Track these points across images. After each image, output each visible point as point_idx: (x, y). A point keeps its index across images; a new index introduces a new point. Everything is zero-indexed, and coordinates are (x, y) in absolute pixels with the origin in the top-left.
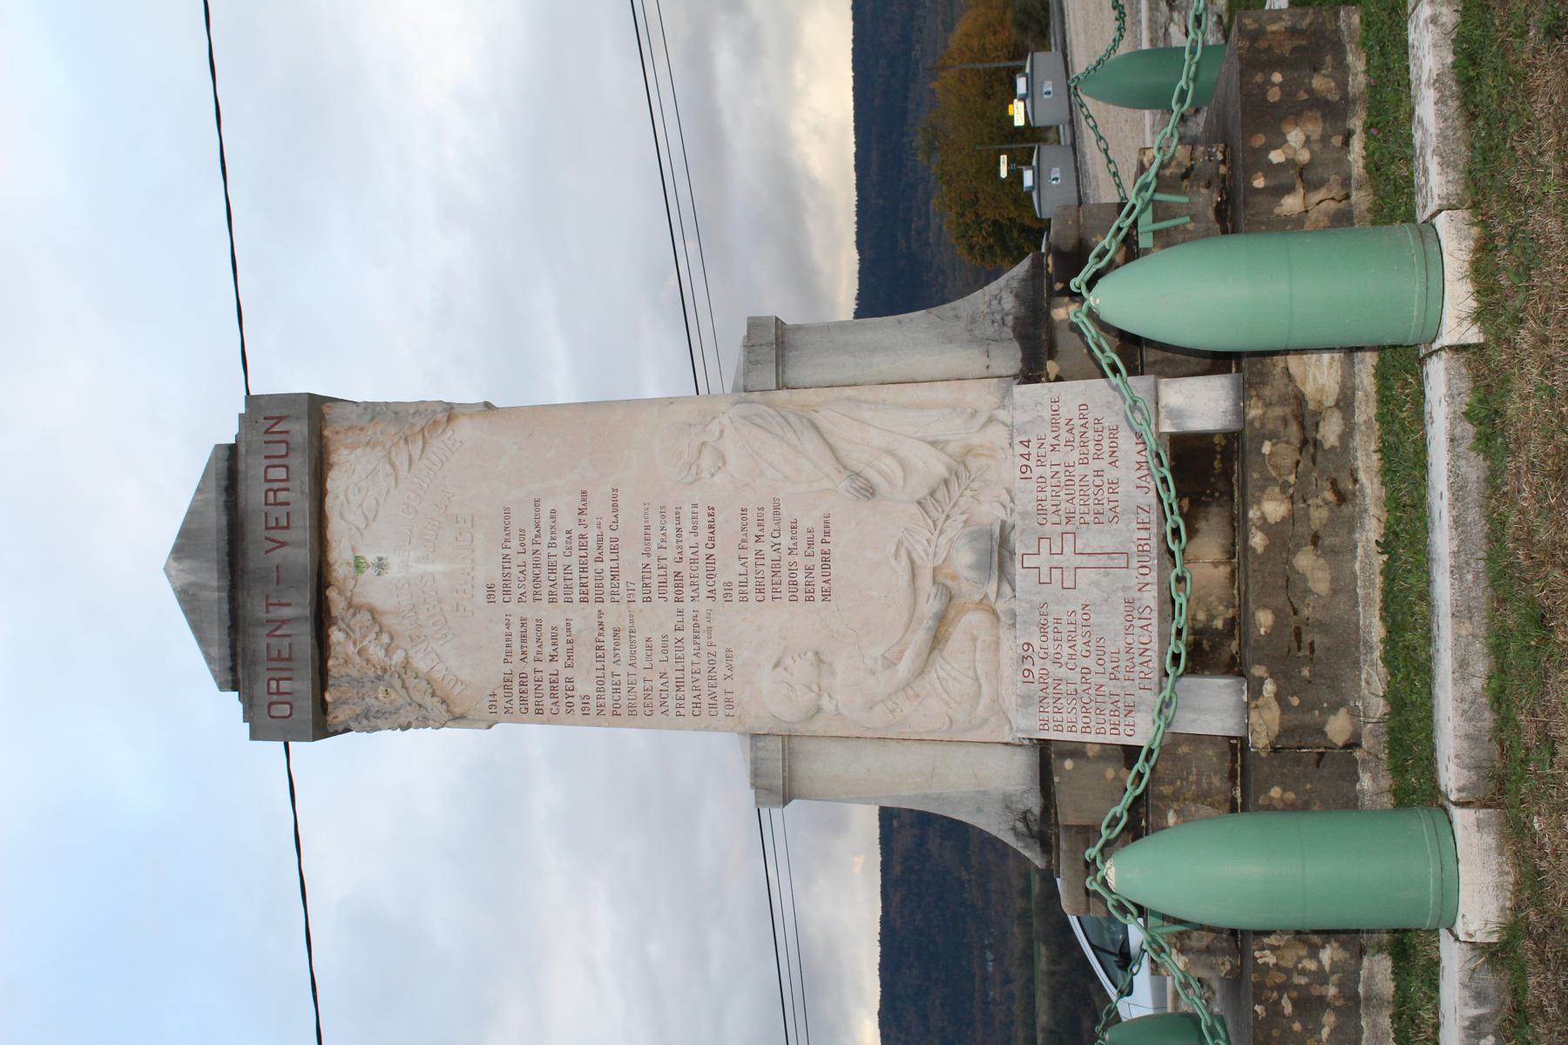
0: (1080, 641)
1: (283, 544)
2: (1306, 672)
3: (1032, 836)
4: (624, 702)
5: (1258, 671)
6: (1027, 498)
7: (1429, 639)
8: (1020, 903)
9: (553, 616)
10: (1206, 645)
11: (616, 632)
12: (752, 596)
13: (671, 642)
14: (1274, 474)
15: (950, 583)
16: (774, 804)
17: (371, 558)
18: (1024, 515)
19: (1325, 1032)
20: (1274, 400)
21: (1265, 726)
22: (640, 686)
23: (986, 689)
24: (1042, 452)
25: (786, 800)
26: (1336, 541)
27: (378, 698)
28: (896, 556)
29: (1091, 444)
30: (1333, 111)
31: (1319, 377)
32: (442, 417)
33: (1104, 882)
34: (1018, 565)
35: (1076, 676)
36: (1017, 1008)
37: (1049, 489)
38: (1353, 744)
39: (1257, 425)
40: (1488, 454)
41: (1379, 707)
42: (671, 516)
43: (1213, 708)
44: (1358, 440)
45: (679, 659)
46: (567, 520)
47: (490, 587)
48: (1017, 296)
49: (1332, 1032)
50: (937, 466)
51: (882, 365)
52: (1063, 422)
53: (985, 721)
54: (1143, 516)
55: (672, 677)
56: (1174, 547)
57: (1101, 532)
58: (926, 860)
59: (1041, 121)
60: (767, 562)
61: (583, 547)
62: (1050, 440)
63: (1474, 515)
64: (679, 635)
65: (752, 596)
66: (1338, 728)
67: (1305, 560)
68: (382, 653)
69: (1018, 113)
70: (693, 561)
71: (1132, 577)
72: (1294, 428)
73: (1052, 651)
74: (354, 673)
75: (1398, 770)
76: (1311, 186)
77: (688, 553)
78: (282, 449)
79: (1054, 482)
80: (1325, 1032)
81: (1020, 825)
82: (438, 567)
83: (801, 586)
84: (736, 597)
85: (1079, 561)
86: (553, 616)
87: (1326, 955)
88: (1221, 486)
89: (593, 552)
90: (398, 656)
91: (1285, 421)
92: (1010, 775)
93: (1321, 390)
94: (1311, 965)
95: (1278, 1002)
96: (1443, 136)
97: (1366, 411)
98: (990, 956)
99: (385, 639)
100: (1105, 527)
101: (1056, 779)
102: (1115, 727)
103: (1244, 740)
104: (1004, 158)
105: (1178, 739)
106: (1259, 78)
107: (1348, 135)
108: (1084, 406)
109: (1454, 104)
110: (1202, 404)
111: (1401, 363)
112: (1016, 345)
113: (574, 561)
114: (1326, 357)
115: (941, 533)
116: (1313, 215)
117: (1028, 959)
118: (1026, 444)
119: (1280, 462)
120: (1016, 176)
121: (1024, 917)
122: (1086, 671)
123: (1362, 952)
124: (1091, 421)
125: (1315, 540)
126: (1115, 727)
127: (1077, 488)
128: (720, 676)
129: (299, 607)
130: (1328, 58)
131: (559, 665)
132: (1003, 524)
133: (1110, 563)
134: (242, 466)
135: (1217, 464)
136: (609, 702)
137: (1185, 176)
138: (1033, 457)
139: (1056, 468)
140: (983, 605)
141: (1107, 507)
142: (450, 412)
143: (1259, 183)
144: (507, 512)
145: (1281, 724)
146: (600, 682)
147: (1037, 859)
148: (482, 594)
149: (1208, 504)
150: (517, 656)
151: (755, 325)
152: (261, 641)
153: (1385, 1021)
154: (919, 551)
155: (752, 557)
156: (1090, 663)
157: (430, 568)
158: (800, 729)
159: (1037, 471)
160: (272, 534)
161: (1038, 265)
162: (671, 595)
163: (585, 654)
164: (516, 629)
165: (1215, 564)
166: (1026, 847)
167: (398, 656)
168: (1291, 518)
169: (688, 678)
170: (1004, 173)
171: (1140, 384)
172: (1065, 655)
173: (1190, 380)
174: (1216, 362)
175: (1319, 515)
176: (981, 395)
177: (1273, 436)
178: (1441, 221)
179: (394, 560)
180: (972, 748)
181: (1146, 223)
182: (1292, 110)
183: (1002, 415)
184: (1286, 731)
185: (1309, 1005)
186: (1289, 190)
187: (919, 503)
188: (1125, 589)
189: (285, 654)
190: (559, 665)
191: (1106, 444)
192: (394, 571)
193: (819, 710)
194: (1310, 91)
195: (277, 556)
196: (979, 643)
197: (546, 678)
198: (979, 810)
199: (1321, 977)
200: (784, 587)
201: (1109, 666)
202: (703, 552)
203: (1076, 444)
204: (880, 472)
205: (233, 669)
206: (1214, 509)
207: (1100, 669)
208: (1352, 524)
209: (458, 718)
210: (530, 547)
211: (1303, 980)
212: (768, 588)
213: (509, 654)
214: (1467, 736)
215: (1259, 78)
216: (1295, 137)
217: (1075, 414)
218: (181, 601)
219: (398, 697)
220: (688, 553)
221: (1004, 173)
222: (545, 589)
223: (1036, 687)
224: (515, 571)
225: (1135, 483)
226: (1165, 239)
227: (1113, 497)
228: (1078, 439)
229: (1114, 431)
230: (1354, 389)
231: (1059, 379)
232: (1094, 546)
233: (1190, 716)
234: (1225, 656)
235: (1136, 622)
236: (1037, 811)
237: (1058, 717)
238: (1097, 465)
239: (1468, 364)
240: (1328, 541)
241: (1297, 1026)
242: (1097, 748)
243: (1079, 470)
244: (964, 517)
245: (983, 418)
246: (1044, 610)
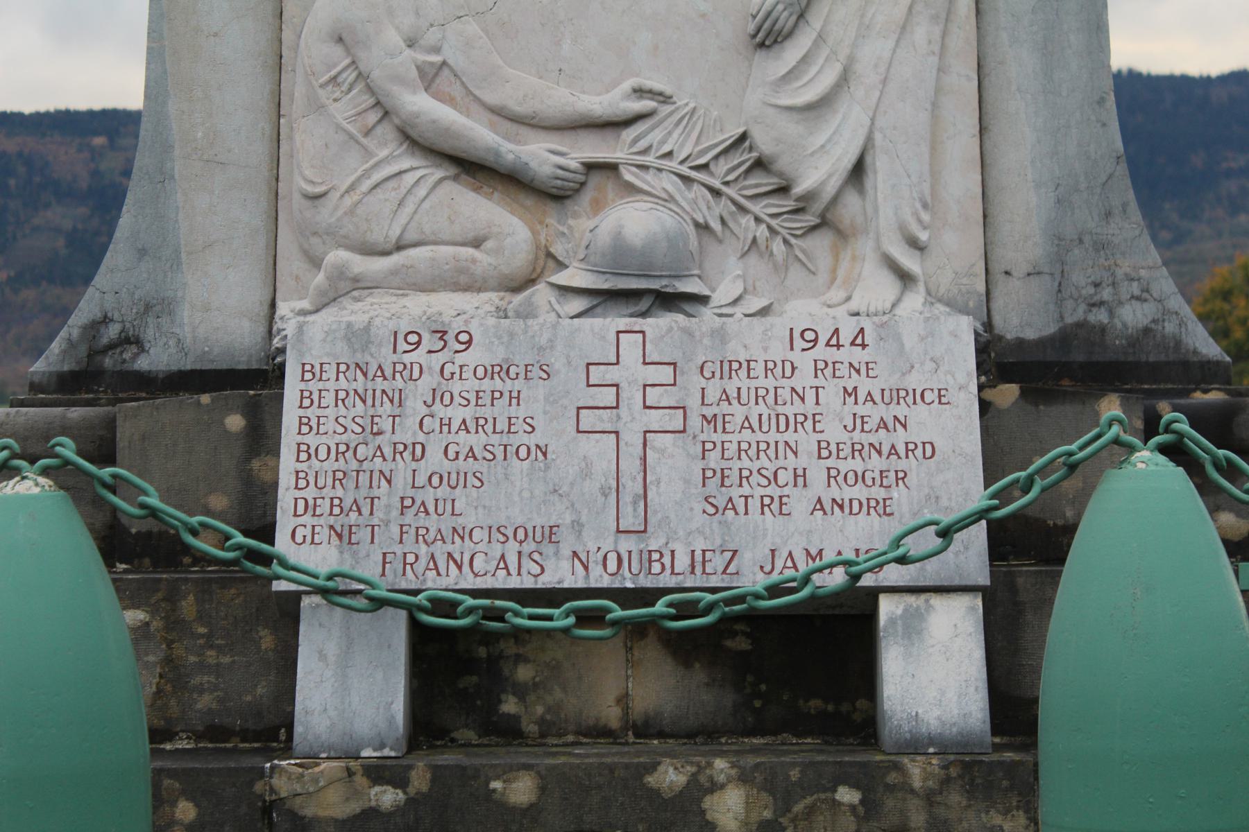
0: (477, 440)
3: (95, 353)
6: (753, 341)
14: (798, 808)
15: (587, 197)
18: (720, 336)
20: (941, 812)
24: (843, 370)
28: (639, 92)
29: (857, 464)
34: (623, 323)
35: (408, 433)
37: (770, 383)
39: (893, 777)
43: (349, 691)
48: (1147, 331)
50: (819, 171)
52: (901, 411)
54: (718, 562)
56: (660, 607)
57: (687, 482)
62: (865, 385)
71: (599, 539)
73: (456, 386)
79: (785, 394)
81: (113, 331)
85: (632, 438)
92: (211, 314)
100: (697, 490)
101: (205, 399)
102: (311, 508)
103: (287, 750)
105: (287, 613)
108: (930, 451)
110: (932, 673)
112: (1051, 329)
115: (686, 179)
118: (859, 341)
122: (418, 452)
124: (902, 464)
126: (311, 508)
127: (772, 437)
132: (702, 300)
133: (627, 498)
135: (815, 704)
138: (832, 354)
139: (810, 396)
141: (735, 492)
145: (316, 820)
147: (51, 360)
154: (653, 135)
159: (805, 362)
161: (1207, 373)
166: (71, 344)
171: (971, 555)
172: (450, 412)
173: (979, 654)
176: (956, 253)
187: (743, 137)
188: (577, 526)
191: (859, 492)
196: (470, 251)
198: (142, 252)
201: (429, 496)
203: (857, 436)
204: (805, 60)
206: (729, 699)
207: (421, 480)
223: (386, 357)
225: (778, 545)
227: (754, 504)
228: (866, 439)
229: (883, 509)
231: (985, 406)
232: (659, 468)
233: (332, 649)
235: (513, 547)
237: (329, 399)
238: (817, 475)
242: (267, 477)
243: (806, 441)
244: (716, 225)
245: (909, 261)
246: (536, 372)
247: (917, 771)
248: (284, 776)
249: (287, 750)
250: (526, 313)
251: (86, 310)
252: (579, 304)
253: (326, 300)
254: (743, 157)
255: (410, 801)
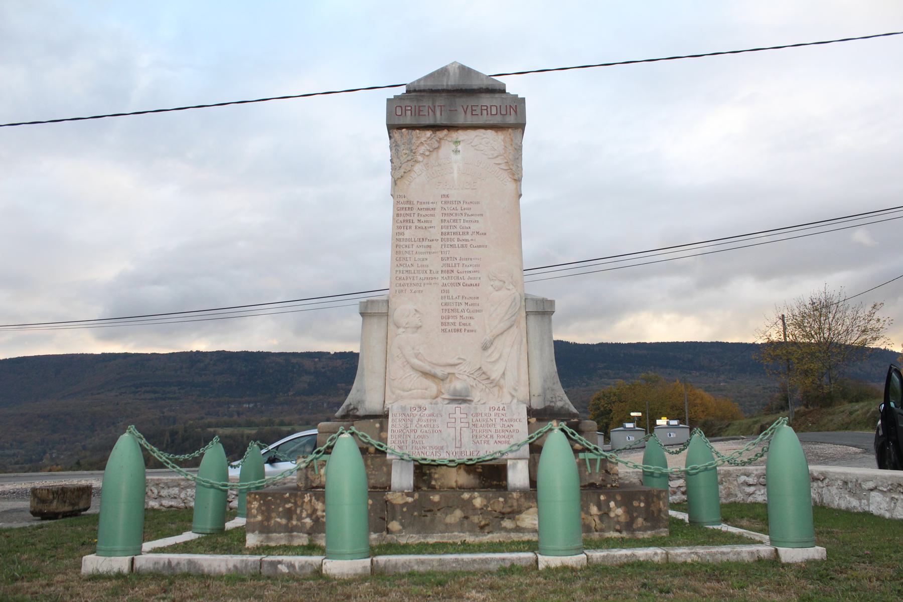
1: (465, 112)
2: (416, 513)
4: (401, 249)
5: (416, 495)
6: (481, 409)
7: (431, 553)
8: (277, 421)
9: (436, 221)
10: (425, 478)
11: (430, 247)
12: (444, 301)
13: (425, 269)
16: (360, 309)
17: (460, 147)
18: (476, 408)
19: (278, 520)
21: (395, 498)
22: (408, 256)
23: (406, 393)
25: (363, 314)
26: (466, 525)
27: (403, 150)
28: (459, 359)
30: (629, 526)
31: (529, 520)
32: (516, 177)
33: (342, 433)
35: (413, 427)
36: (225, 418)
38: (388, 531)
40: (499, 571)
41: (403, 541)
42: (477, 269)
44: (504, 534)
45: (419, 272)
46: (474, 227)
47: (447, 196)
49: (279, 523)
50: (495, 375)
51: (535, 353)
53: (393, 393)
54: (475, 453)
55: (412, 269)
58: (344, 368)
59: (657, 432)
60: (457, 307)
61: (464, 233)
63: (476, 566)
64: (428, 272)
65: (444, 301)
66: (395, 525)
67: (458, 513)
68: (421, 152)
69: (662, 422)
70: (458, 278)
71: (452, 449)
72: (508, 510)
74: (413, 141)
75: (380, 547)
76: (601, 517)
77: (461, 275)
78: (504, 112)
80: (278, 520)
81: (352, 407)
82: (456, 175)
83: (447, 321)
84: (443, 295)
86: (436, 221)
87: (308, 521)
88: (487, 484)
89: (461, 237)
90: (420, 158)
91: (512, 506)
93: (523, 520)
94: (304, 515)
95: (290, 502)
96: (614, 557)
97: (515, 537)
98: (251, 405)
99: (427, 153)
104: (640, 414)
106: (642, 498)
107: (620, 531)
108: (518, 431)
109: (625, 560)
110: (518, 476)
111: (533, 546)
112: (542, 407)
113: (458, 230)
114: (536, 522)
116: (590, 518)
117: (249, 425)
118: (504, 409)
119: (496, 504)
120: (631, 420)
121: (271, 423)
122: (416, 431)
123: (309, 534)
125: (466, 518)
128: (412, 288)
129: (440, 119)
130: (649, 524)
131: (416, 224)
134: (497, 95)
136: (402, 243)
137: (607, 471)
140: (440, 393)
142: (518, 181)
143: (602, 498)
144: (478, 203)
146: (410, 240)
147: (340, 412)
148: (444, 192)
149: (479, 479)
150: (420, 206)
151: (552, 303)
152: (426, 103)
153: (283, 542)
154: (462, 367)
155: (459, 301)
156: (419, 433)
157: (455, 171)
158: (390, 320)
160: (470, 108)
161: (574, 416)
162: (444, 269)
163: (420, 234)
164: (431, 206)
165: (456, 482)
167: (420, 158)
168: (474, 508)
169: (411, 275)
170: (633, 414)
174: (533, 483)
175: (475, 519)
176: (523, 392)
177: (506, 502)
178: (584, 556)
179: (459, 157)
180: (382, 388)
181: (588, 456)
182: (630, 511)
183: (515, 401)
184: (393, 506)
185: (289, 514)
186: (599, 509)
188: (447, 447)
189: (421, 113)
190: (416, 224)
191: (503, 439)
192: (454, 157)
193: (398, 327)
194: (637, 517)
195: (461, 110)
197: (411, 218)
198: (358, 391)
199: (300, 518)
200: (447, 314)
202: (461, 281)
205: (415, 91)
206: (478, 481)
208: (472, 531)
209: (395, 182)
210: (463, 212)
211: (298, 511)
212: (447, 307)
213: (421, 203)
214: (396, 564)
215: (642, 498)
216: (620, 511)
217: (515, 428)
218: (442, 69)
219: (404, 158)
220: (461, 275)
221: (633, 414)
222: (447, 218)
223: (409, 412)
224: (454, 206)
225: (486, 450)
226: (581, 464)
230: (523, 533)
231: (529, 423)
234: (421, 485)
236: (358, 413)
239: (531, 565)
240: (466, 522)
241: (281, 509)
245: (514, 393)
247: (515, 495)
248: (390, 496)
249: (390, 490)
250: (436, 404)
251: (346, 403)
252: (447, 402)
253: (396, 400)
254: (480, 372)
255: (415, 501)
